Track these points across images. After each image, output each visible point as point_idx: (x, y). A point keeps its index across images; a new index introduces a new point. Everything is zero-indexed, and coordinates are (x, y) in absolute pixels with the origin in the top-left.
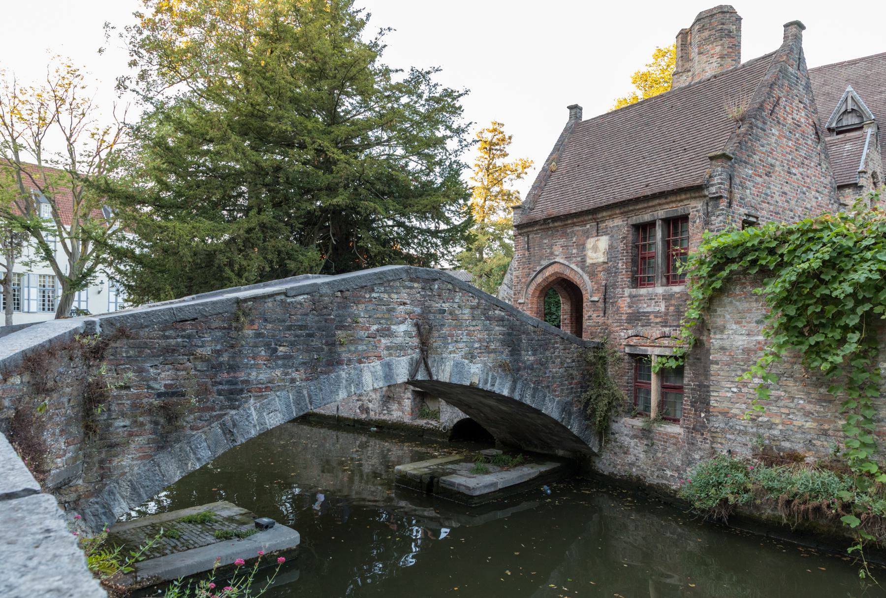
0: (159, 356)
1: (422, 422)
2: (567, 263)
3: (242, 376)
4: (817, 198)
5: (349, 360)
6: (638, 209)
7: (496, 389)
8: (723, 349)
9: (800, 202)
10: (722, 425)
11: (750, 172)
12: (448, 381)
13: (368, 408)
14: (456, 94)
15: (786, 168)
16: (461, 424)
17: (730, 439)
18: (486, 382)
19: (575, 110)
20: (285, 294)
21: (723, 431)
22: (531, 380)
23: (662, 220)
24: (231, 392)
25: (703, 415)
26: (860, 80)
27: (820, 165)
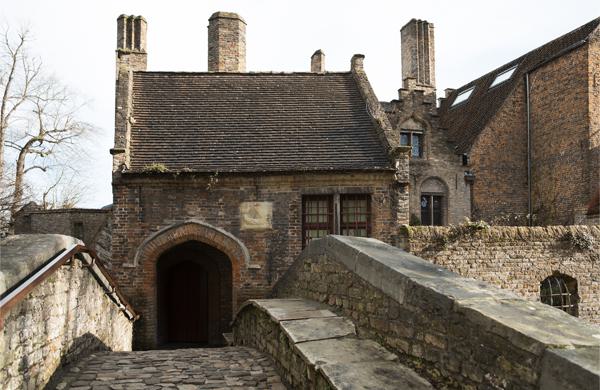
2: (211, 226)
23: (341, 195)
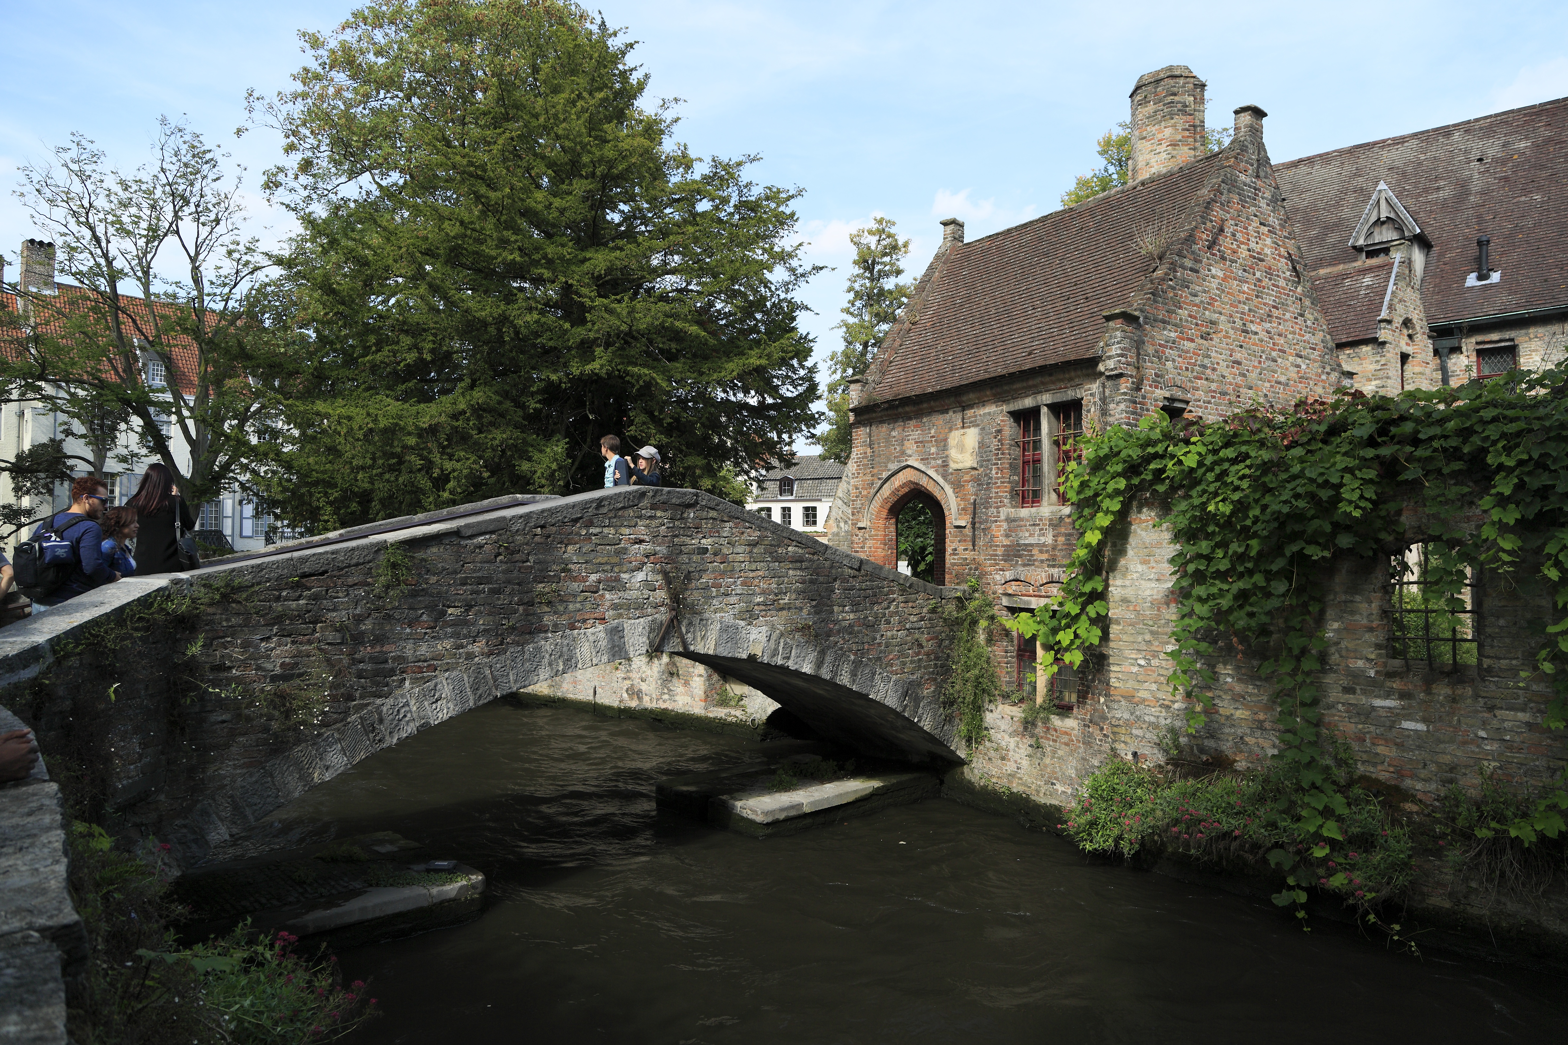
0: (273, 625)
1: (719, 713)
2: (923, 468)
3: (391, 650)
4: (1299, 366)
5: (555, 625)
6: (1016, 390)
7: (791, 665)
8: (1125, 600)
9: (1267, 374)
10: (1126, 716)
11: (1173, 335)
12: (711, 652)
13: (640, 691)
14: (783, 195)
15: (1239, 324)
16: (775, 713)
17: (1137, 736)
18: (775, 653)
19: (952, 227)
20: (456, 533)
21: (1128, 724)
22: (850, 651)
24: (377, 673)
25: (1102, 700)
26: (1409, 169)
27: (1302, 315)
